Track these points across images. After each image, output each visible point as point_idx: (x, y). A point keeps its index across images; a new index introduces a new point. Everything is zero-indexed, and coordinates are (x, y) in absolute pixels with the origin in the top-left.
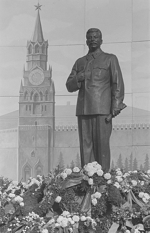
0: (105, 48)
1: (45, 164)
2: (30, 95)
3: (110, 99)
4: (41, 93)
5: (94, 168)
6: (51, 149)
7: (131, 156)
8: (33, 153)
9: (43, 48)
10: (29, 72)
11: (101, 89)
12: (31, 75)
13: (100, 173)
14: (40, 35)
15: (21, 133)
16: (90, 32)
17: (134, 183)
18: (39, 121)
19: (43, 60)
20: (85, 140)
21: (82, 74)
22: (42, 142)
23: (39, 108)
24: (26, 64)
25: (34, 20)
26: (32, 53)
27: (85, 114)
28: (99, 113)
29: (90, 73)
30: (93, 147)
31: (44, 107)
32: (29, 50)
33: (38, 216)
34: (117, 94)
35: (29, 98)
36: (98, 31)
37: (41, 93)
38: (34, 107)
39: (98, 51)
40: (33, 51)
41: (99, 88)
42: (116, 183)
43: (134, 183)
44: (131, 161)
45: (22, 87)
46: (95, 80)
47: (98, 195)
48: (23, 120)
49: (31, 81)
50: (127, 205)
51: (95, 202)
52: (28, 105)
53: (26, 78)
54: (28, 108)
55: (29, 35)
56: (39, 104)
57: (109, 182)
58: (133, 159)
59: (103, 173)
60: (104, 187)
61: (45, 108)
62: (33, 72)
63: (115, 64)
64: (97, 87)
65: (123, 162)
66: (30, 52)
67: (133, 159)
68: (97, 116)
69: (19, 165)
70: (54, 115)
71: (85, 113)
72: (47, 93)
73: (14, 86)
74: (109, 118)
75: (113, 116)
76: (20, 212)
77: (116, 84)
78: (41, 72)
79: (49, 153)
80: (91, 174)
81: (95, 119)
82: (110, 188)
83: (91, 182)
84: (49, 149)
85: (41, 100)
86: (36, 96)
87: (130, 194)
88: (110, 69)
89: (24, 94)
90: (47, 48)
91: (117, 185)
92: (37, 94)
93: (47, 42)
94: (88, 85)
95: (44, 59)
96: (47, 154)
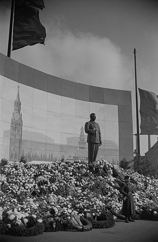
1: (18, 154)
4: (18, 123)
9: (19, 104)
16: (91, 115)
18: (17, 135)
19: (19, 110)
22: (17, 145)
23: (17, 129)
27: (97, 143)
37: (18, 123)
55: (15, 98)
61: (19, 130)
65: (42, 156)
66: (15, 105)
78: (18, 114)
79: (19, 149)
84: (19, 148)
92: (16, 124)
93: (21, 103)
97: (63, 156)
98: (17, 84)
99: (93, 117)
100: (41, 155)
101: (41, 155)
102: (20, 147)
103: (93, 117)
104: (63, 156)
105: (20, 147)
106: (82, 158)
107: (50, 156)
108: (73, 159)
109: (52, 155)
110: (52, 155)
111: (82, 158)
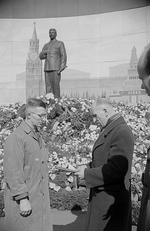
0: (57, 38)
2: (31, 65)
3: (60, 63)
4: (36, 64)
5: (51, 96)
6: (41, 90)
7: (77, 93)
8: (32, 91)
9: (37, 43)
10: (30, 54)
11: (55, 58)
12: (31, 55)
13: (53, 98)
14: (35, 36)
15: (27, 83)
17: (69, 103)
18: (35, 77)
20: (48, 83)
21: (46, 51)
23: (35, 71)
24: (29, 50)
25: (33, 30)
26: (32, 45)
28: (53, 69)
29: (50, 50)
30: (52, 86)
31: (37, 70)
32: (30, 43)
33: (22, 119)
34: (63, 60)
35: (30, 66)
36: (54, 30)
37: (36, 64)
38: (33, 70)
39: (54, 40)
40: (32, 44)
41: (54, 58)
42: (59, 103)
43: (69, 103)
44: (76, 95)
45: (27, 61)
46: (52, 53)
47: (51, 108)
48: (28, 76)
49: (31, 58)
50: (65, 113)
51: (49, 112)
52: (30, 69)
53: (29, 57)
54: (30, 71)
55: (30, 36)
56: (35, 69)
57: (56, 102)
58: (78, 94)
59: (54, 98)
60: (54, 105)
62: (32, 54)
63: (62, 46)
64: (53, 57)
65: (73, 95)
66: (31, 45)
67: (78, 94)
68: (53, 71)
69: (26, 96)
70: (42, 74)
71: (47, 70)
72: (39, 64)
73: (24, 60)
74: (59, 72)
75: (61, 71)
76: (14, 117)
77: (63, 55)
80: (48, 99)
81: (52, 73)
82: (57, 105)
83: (48, 102)
84: (40, 90)
85: (36, 67)
86: (34, 65)
87: (66, 108)
88: (59, 48)
89: (28, 64)
90: (39, 42)
91: (60, 104)
93: (39, 40)
94: (49, 56)
95: (37, 48)
96: (39, 92)
97: (104, 93)
98: (33, 20)
99: (53, 35)
100: (72, 94)
101: (72, 94)
102: (40, 88)
103: (53, 35)
104: (104, 93)
105: (40, 88)
106: (134, 92)
107: (85, 95)
108: (119, 94)
109: (87, 93)
110: (87, 93)
111: (134, 92)
